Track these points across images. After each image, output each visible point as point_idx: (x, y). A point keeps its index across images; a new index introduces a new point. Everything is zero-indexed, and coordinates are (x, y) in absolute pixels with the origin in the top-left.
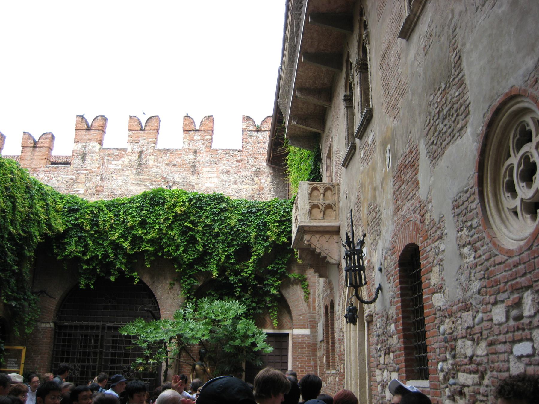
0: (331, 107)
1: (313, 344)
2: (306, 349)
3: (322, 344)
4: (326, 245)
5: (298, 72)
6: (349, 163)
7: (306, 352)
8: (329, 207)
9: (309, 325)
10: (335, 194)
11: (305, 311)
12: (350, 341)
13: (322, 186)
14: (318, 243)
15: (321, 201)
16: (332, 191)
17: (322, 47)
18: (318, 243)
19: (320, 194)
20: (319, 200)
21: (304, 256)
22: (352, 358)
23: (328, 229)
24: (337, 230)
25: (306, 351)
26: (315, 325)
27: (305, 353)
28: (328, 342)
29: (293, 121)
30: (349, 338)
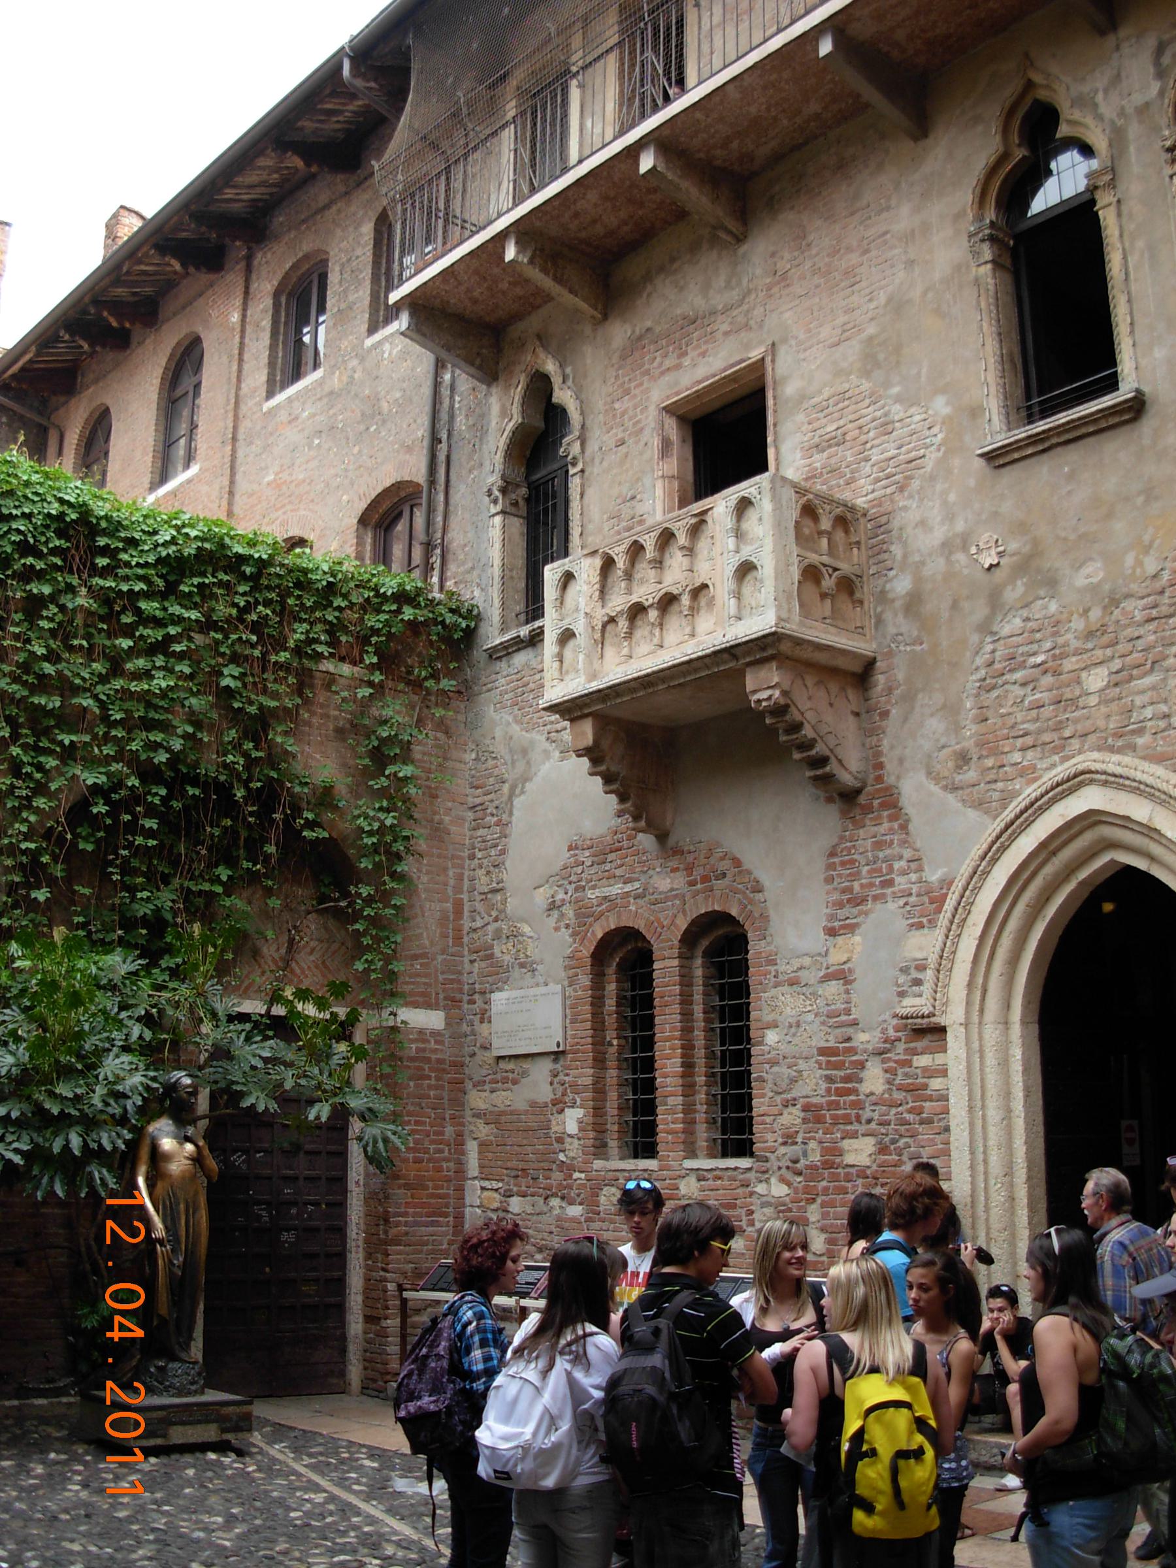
0: (740, 239)
1: (454, 1064)
2: (433, 1082)
3: (544, 1068)
4: (828, 717)
5: (730, 87)
6: (1044, 451)
7: (432, 1093)
8: (848, 586)
9: (441, 996)
10: (858, 543)
11: (432, 944)
12: (982, 1057)
13: (827, 507)
14: (809, 705)
15: (825, 559)
16: (847, 531)
17: (900, 35)
18: (809, 705)
19: (820, 533)
20: (816, 552)
21: (605, 744)
22: (994, 1114)
23: (841, 662)
24: (857, 668)
25: (430, 1087)
26: (458, 996)
27: (429, 1097)
28: (599, 1062)
29: (518, 253)
30: (976, 1045)
